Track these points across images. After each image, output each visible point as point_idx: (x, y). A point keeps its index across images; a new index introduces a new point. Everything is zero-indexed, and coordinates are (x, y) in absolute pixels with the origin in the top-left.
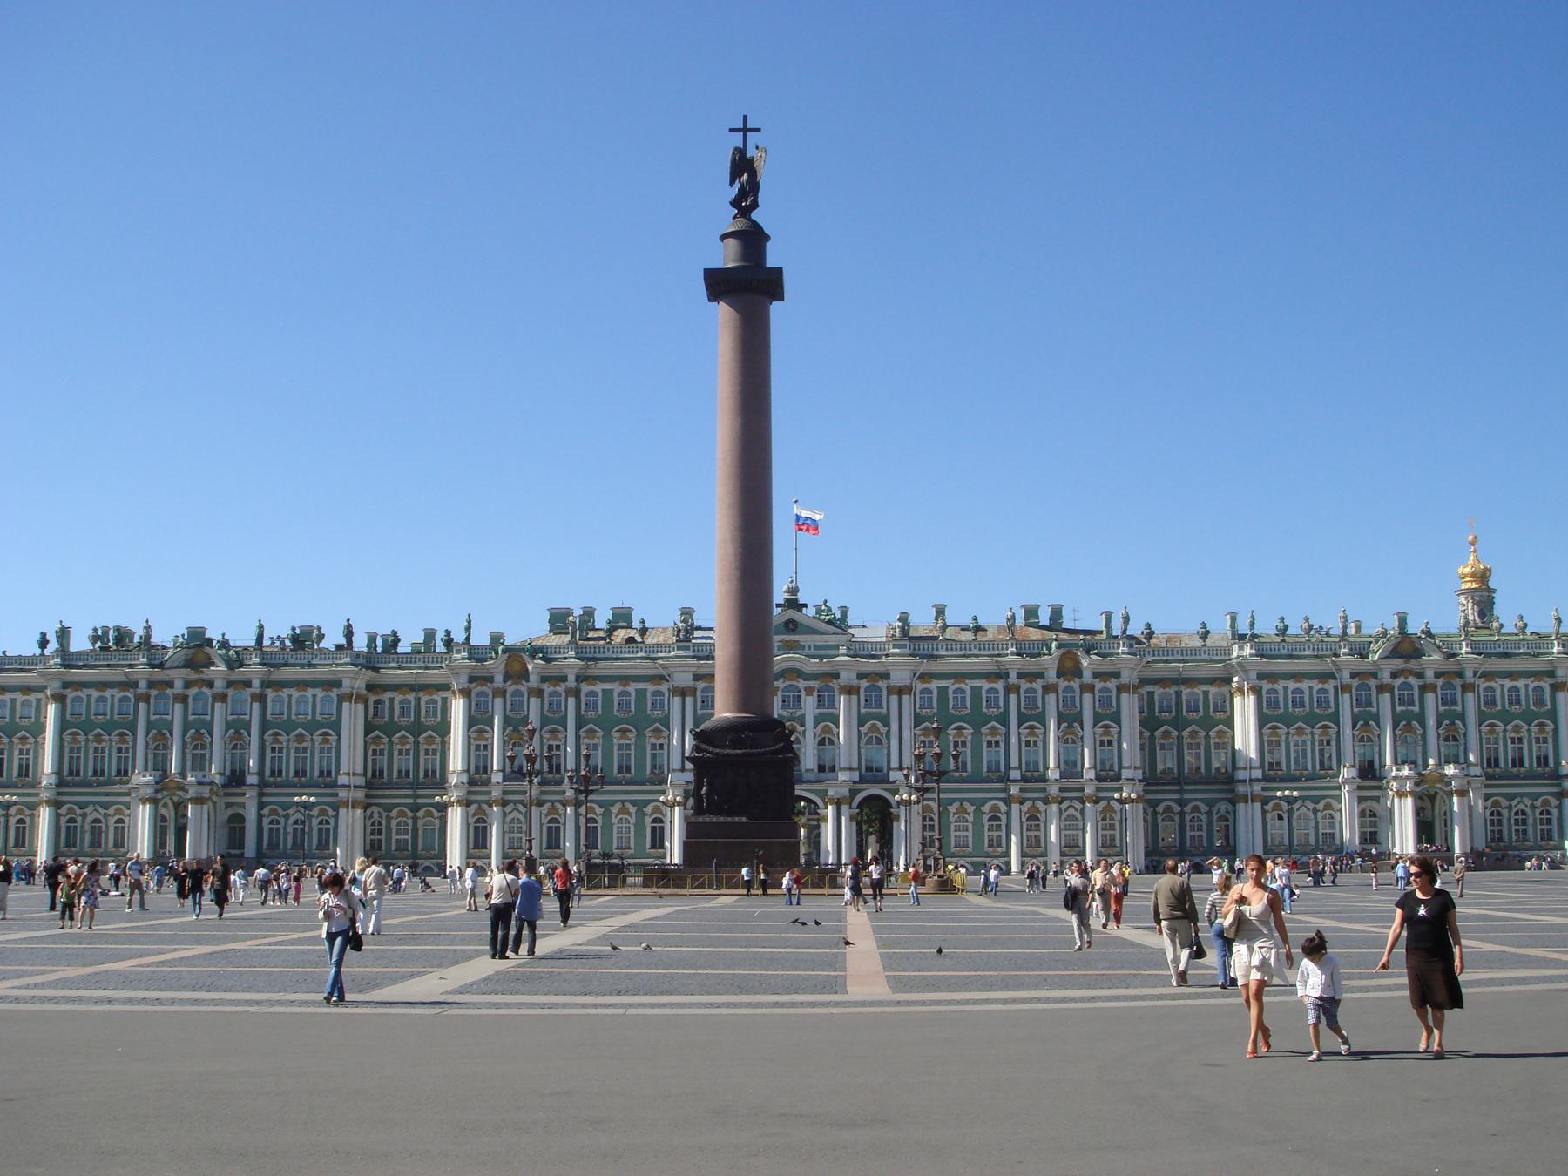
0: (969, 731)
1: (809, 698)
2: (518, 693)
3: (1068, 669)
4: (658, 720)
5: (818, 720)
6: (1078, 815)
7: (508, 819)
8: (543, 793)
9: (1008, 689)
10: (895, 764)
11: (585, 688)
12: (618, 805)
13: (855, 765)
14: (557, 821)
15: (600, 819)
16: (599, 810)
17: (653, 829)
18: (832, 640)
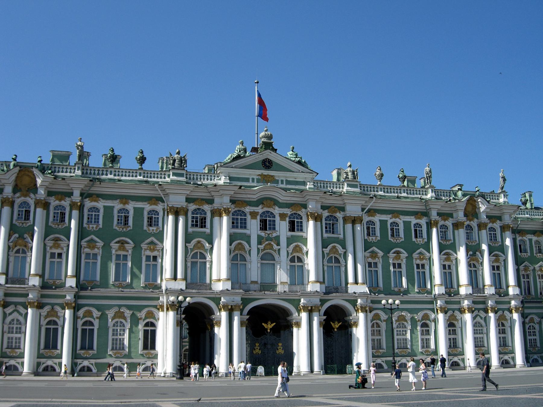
0: (404, 255)
1: (283, 223)
2: (25, 204)
3: (471, 211)
4: (154, 235)
5: (290, 240)
6: (482, 322)
7: (9, 319)
8: (43, 296)
9: (430, 225)
10: (351, 279)
11: (88, 204)
12: (116, 309)
13: (322, 280)
14: (55, 323)
15: (96, 323)
16: (96, 313)
17: (146, 332)
18: (300, 177)
